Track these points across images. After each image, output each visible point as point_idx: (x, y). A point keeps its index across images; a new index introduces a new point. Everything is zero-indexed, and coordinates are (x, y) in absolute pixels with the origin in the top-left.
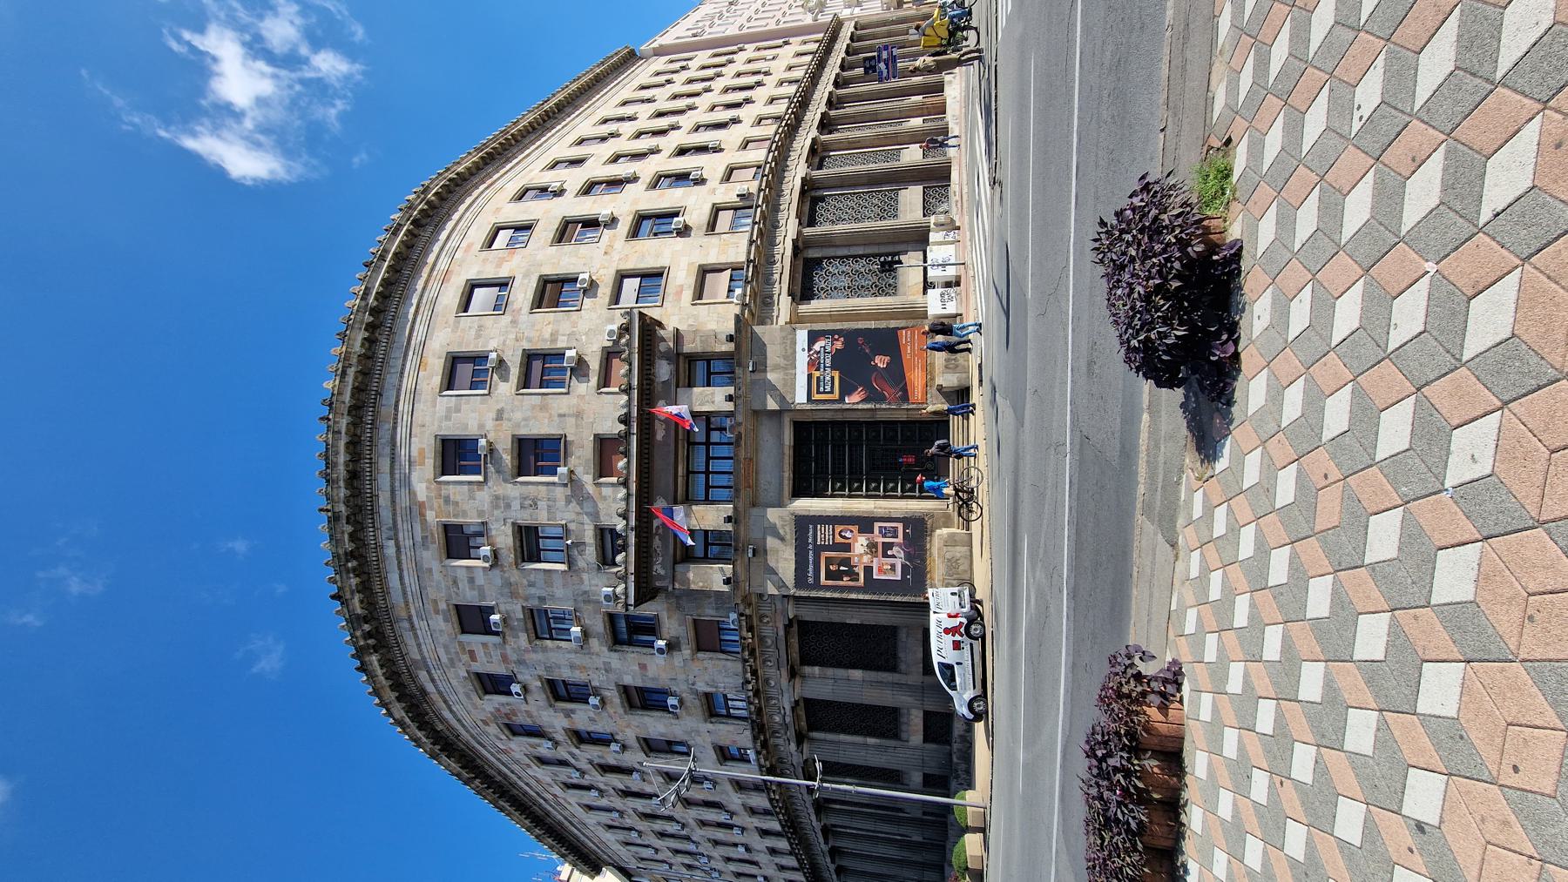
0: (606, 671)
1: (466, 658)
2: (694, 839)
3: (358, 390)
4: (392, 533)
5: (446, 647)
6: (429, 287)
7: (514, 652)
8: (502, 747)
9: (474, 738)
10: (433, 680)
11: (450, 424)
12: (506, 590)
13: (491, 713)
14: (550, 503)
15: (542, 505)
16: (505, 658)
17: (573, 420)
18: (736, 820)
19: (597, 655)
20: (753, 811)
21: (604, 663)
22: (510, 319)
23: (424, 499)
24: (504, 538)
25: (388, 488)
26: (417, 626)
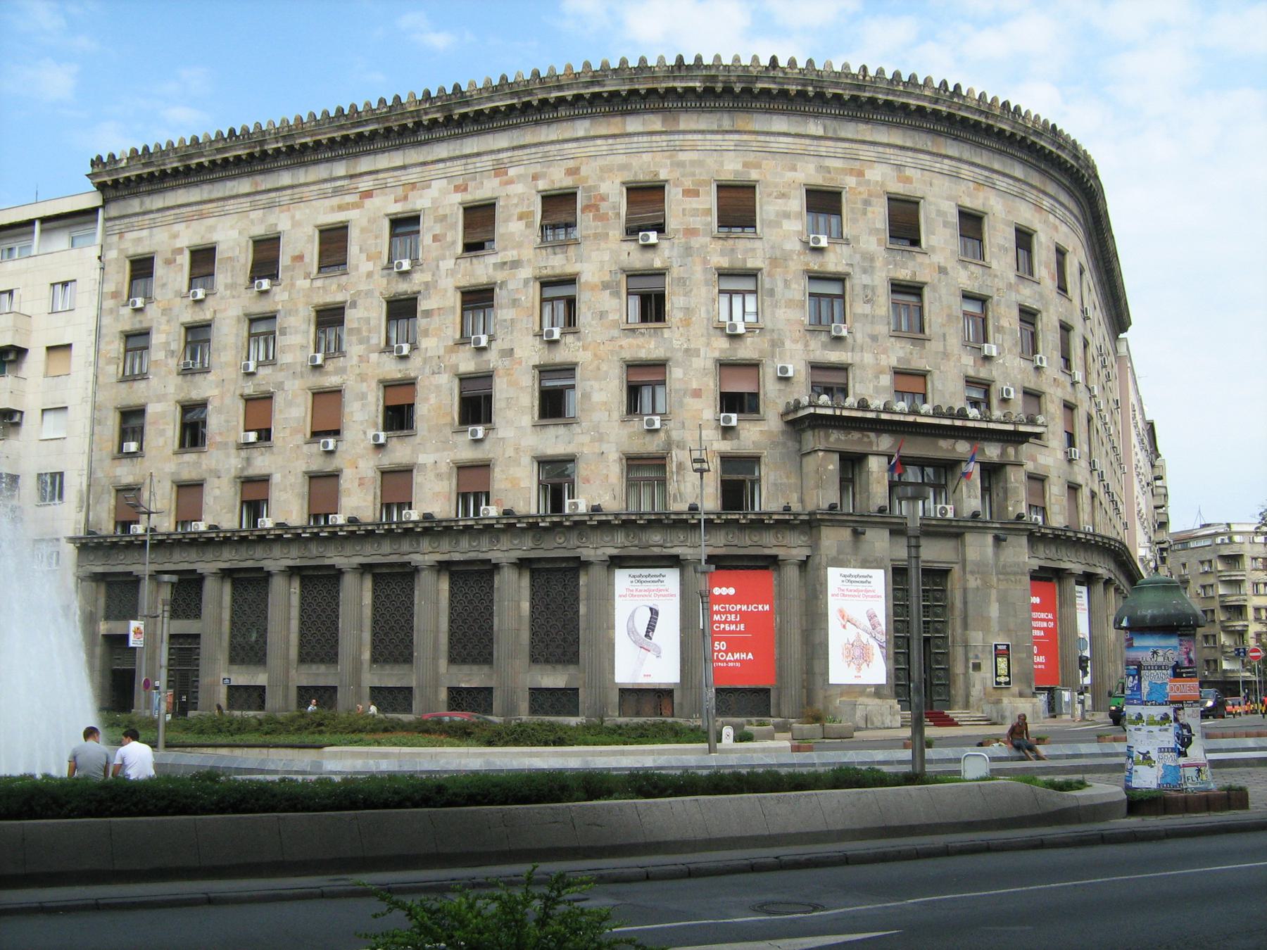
0: (687, 350)
1: (688, 184)
3: (964, 120)
4: (830, 135)
5: (700, 163)
8: (512, 172)
11: (933, 215)
12: (778, 254)
13: (596, 187)
14: (870, 317)
15: (867, 309)
16: (691, 232)
17: (941, 349)
19: (708, 344)
22: (1013, 282)
23: (867, 177)
24: (834, 262)
26: (727, 137)
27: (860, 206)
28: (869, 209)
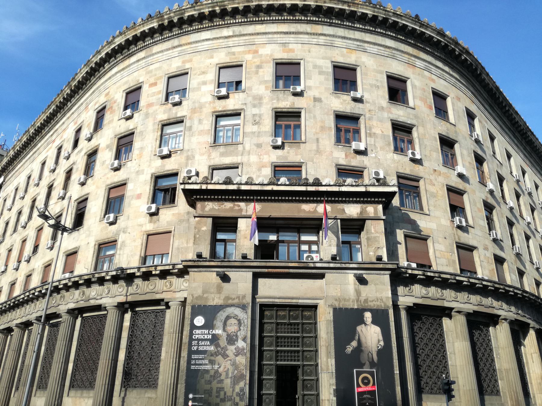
0: (138, 172)
1: (152, 80)
2: (14, 235)
4: (237, 33)
5: (160, 68)
6: (403, 55)
7: (154, 111)
8: (90, 106)
9: (97, 88)
10: (138, 61)
12: (197, 105)
13: (113, 98)
14: (256, 134)
15: (255, 128)
16: (150, 105)
17: (314, 147)
18: (23, 264)
19: (149, 166)
20: (29, 276)
21: (143, 170)
23: (260, 53)
25: (267, 31)
27: (254, 69)
28: (261, 70)
